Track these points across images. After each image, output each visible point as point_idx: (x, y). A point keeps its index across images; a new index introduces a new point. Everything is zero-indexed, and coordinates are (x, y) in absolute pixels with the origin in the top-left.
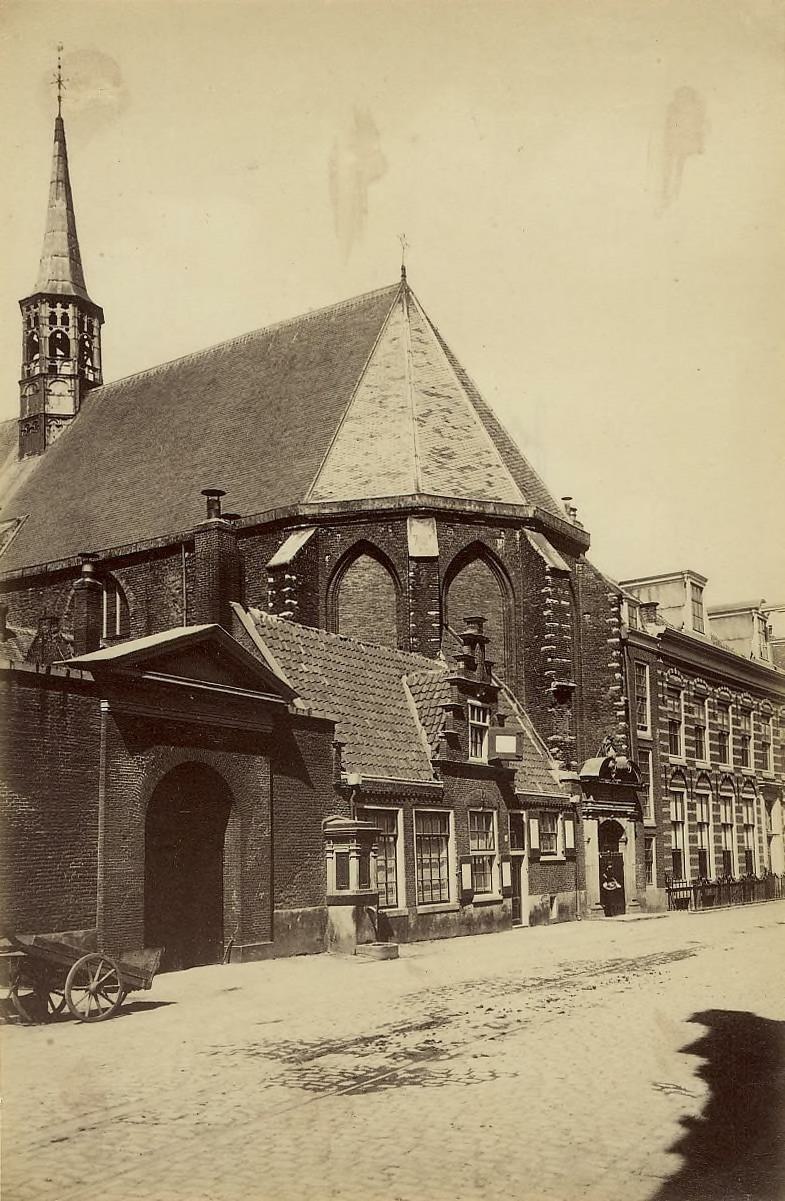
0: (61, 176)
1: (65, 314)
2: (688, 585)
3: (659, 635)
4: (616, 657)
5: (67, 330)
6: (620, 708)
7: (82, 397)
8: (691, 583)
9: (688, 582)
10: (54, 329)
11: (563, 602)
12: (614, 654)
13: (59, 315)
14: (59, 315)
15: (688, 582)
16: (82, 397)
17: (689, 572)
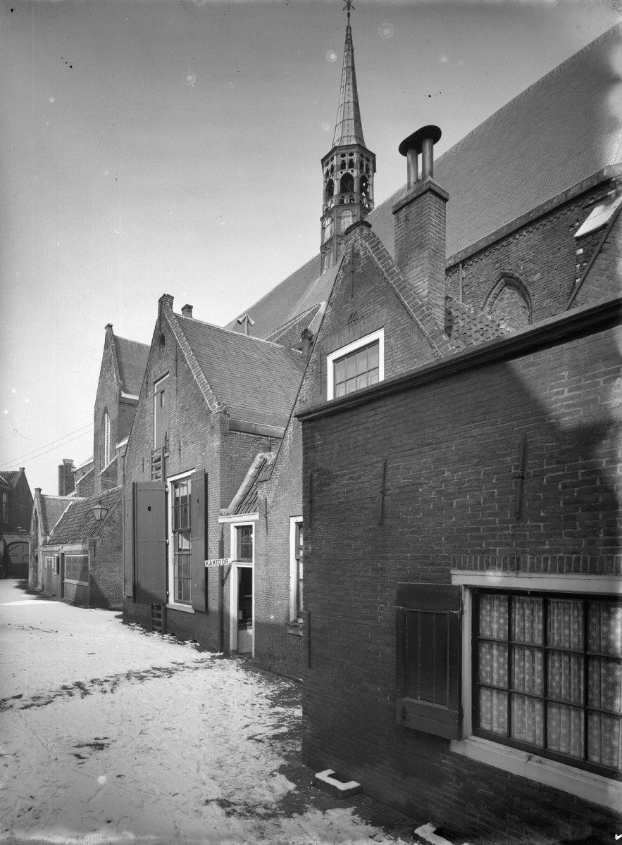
0: (350, 64)
1: (351, 161)
5: (352, 171)
13: (347, 162)
14: (347, 162)
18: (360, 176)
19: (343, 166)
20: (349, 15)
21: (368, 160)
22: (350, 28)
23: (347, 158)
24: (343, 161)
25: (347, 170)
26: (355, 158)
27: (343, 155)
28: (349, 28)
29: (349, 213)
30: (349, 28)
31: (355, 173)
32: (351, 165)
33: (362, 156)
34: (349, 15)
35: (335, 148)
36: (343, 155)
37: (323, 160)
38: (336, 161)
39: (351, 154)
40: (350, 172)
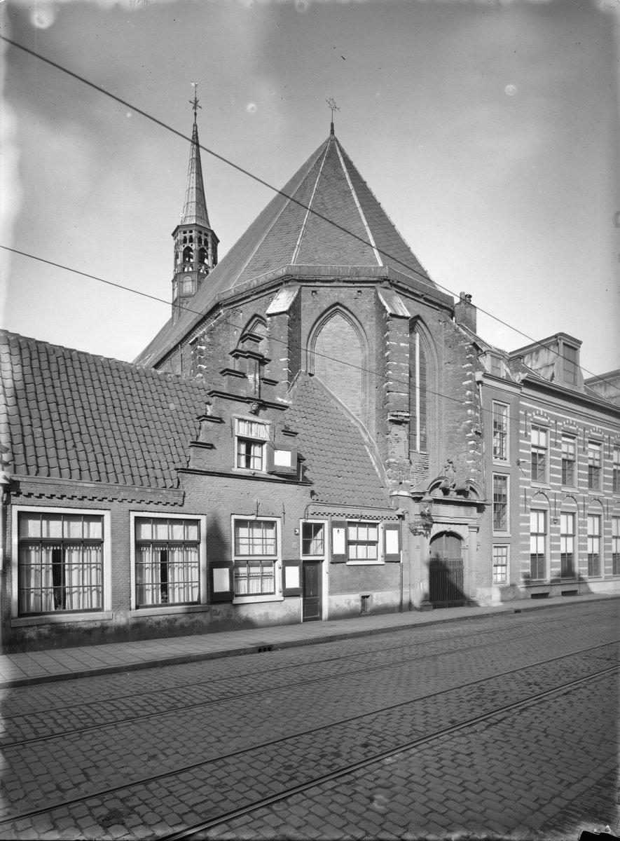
1: (191, 236)
2: (561, 345)
3: (524, 381)
4: (470, 396)
6: (471, 439)
7: (199, 282)
8: (564, 344)
9: (561, 343)
10: (186, 246)
11: (402, 344)
12: (468, 393)
13: (188, 237)
14: (188, 237)
15: (561, 343)
16: (199, 282)
17: (562, 334)
18: (198, 248)
19: (185, 241)
20: (196, 114)
21: (206, 235)
22: (196, 125)
23: (188, 235)
24: (185, 237)
25: (188, 244)
26: (194, 234)
27: (185, 232)
28: (195, 125)
29: (189, 278)
30: (195, 125)
31: (194, 246)
32: (191, 240)
33: (200, 232)
34: (196, 114)
35: (178, 227)
36: (185, 232)
37: (173, 235)
38: (180, 236)
39: (191, 232)
40: (190, 245)
